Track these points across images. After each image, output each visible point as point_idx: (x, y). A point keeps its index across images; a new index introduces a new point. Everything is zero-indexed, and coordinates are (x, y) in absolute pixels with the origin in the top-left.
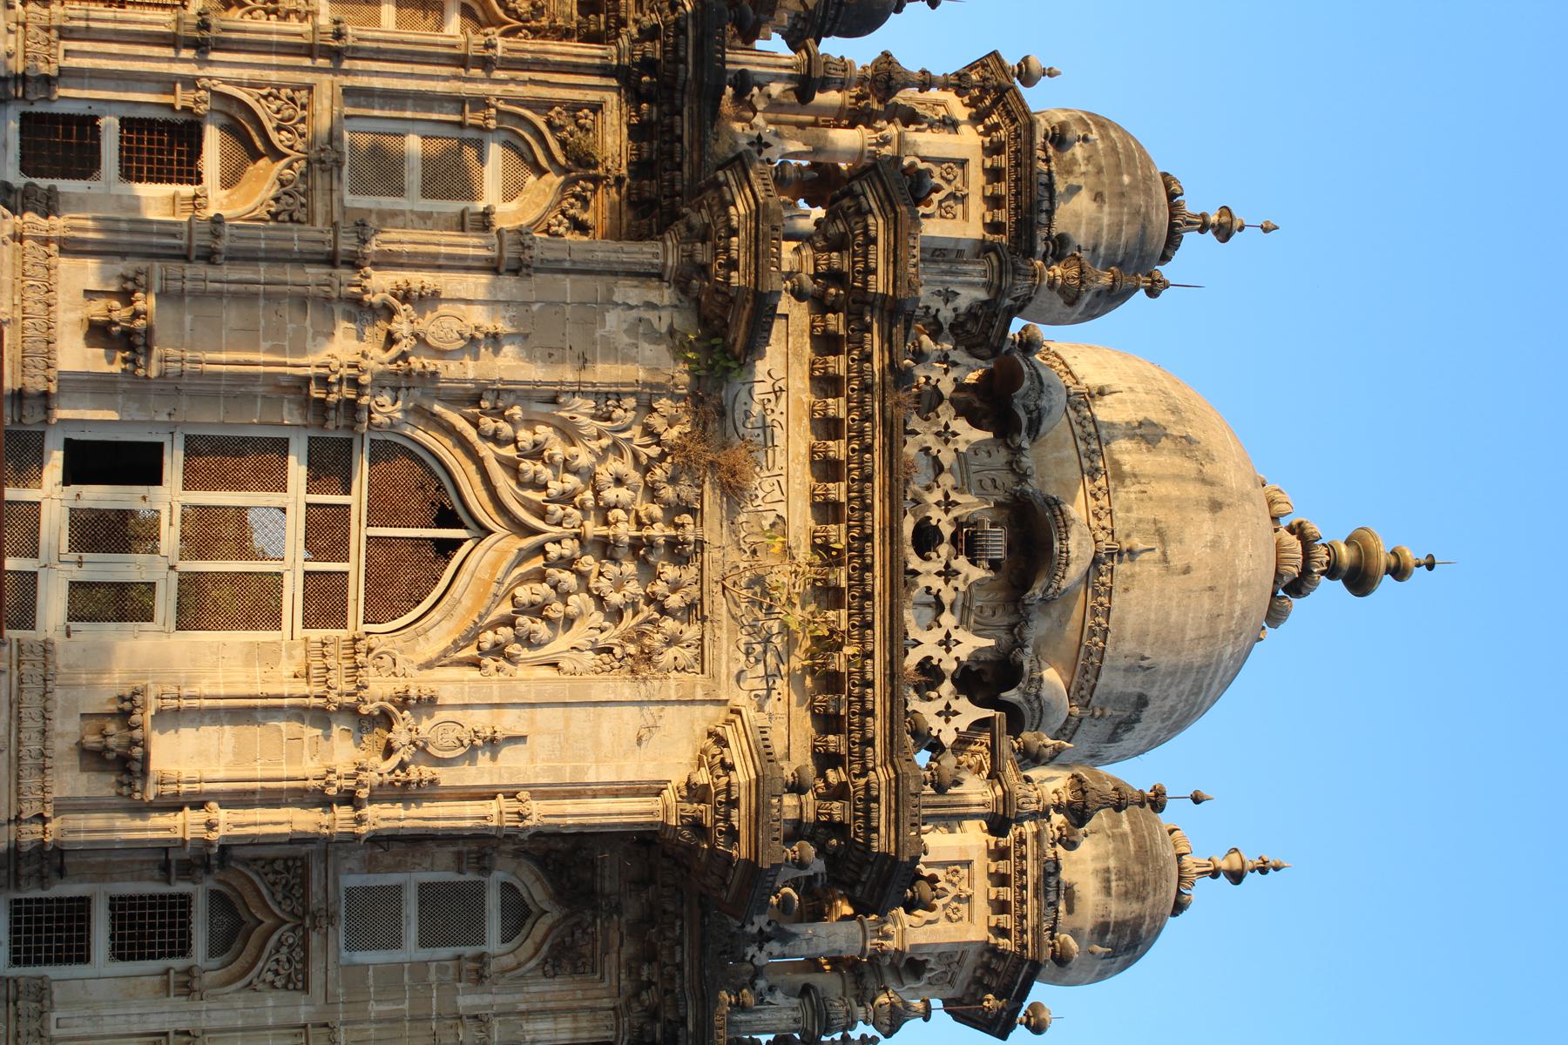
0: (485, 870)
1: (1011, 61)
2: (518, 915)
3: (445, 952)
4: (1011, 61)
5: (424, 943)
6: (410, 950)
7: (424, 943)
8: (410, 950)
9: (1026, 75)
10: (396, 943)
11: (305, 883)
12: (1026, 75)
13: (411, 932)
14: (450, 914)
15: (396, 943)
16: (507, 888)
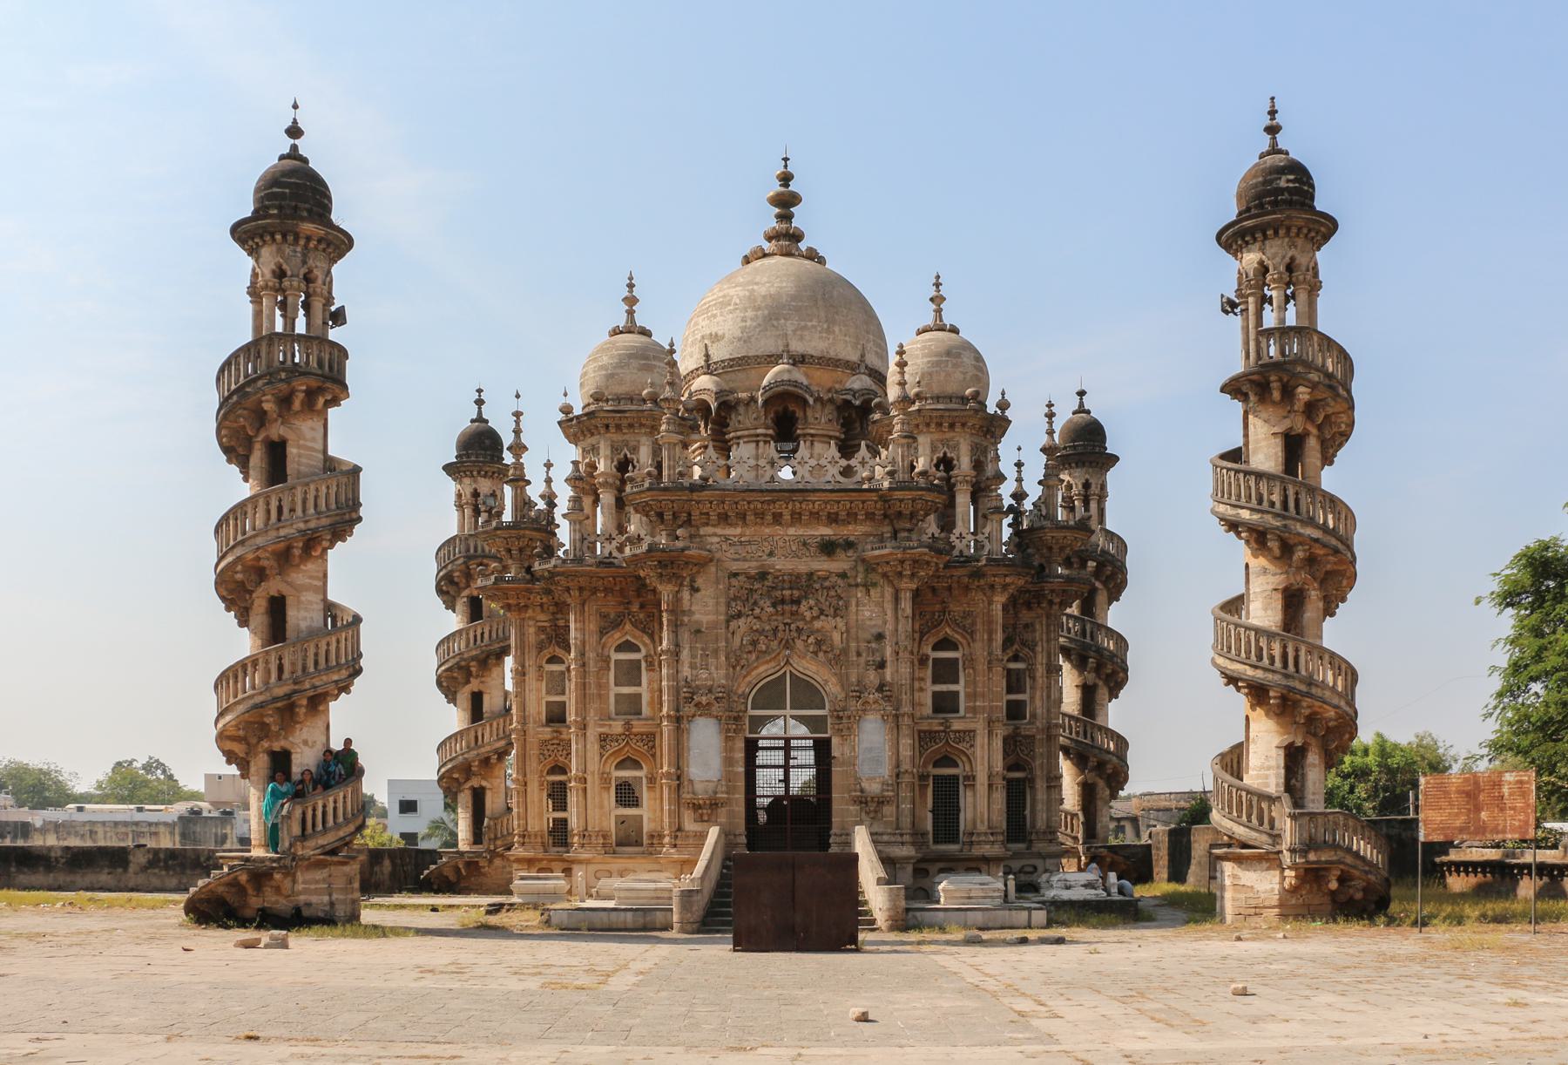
0: (927, 657)
1: (561, 416)
2: (945, 644)
3: (961, 674)
4: (561, 416)
5: (956, 682)
6: (960, 687)
7: (956, 682)
8: (960, 687)
9: (566, 410)
10: (957, 693)
11: (930, 732)
12: (566, 410)
13: (953, 687)
14: (946, 671)
15: (957, 693)
16: (935, 648)
